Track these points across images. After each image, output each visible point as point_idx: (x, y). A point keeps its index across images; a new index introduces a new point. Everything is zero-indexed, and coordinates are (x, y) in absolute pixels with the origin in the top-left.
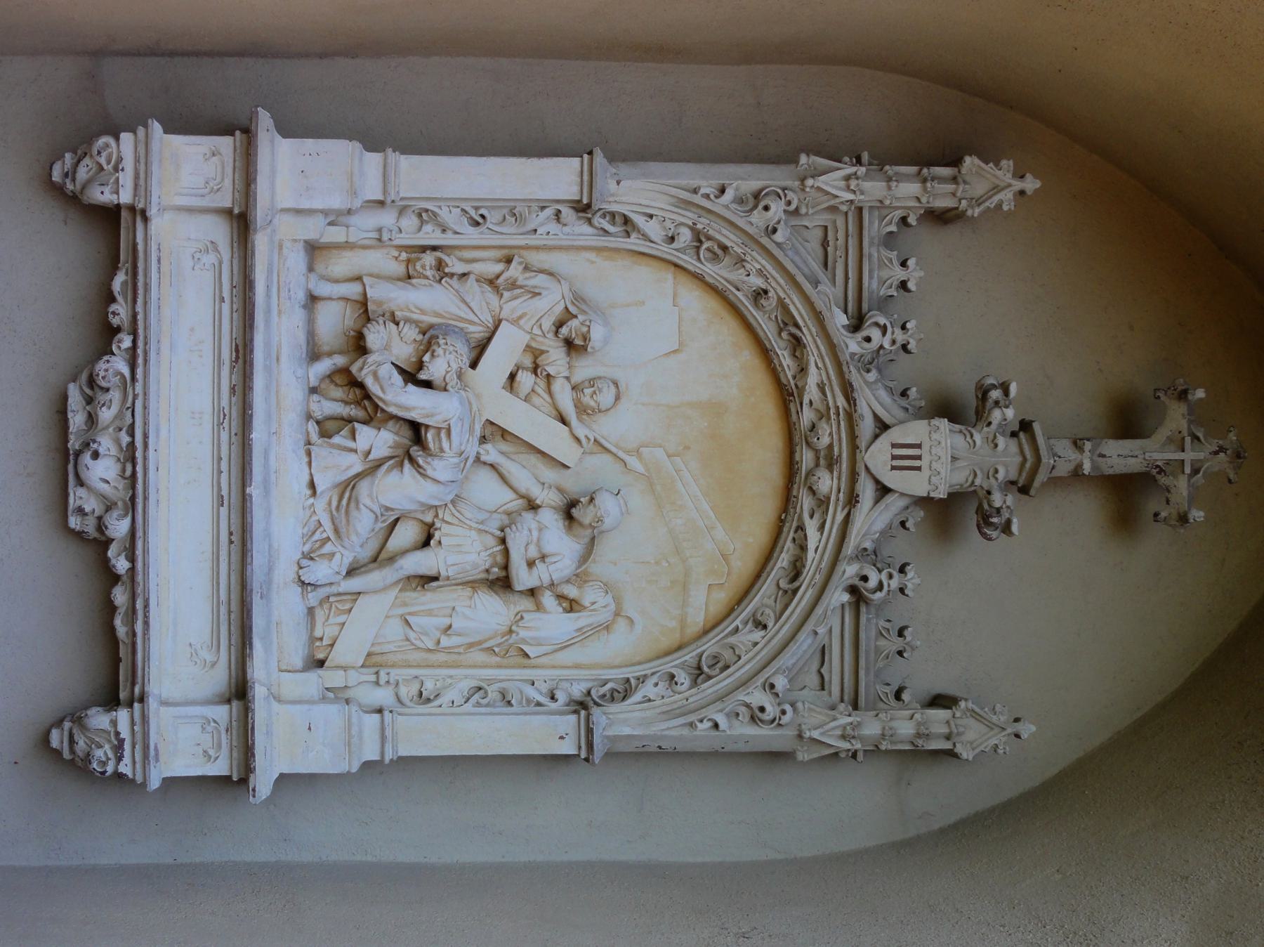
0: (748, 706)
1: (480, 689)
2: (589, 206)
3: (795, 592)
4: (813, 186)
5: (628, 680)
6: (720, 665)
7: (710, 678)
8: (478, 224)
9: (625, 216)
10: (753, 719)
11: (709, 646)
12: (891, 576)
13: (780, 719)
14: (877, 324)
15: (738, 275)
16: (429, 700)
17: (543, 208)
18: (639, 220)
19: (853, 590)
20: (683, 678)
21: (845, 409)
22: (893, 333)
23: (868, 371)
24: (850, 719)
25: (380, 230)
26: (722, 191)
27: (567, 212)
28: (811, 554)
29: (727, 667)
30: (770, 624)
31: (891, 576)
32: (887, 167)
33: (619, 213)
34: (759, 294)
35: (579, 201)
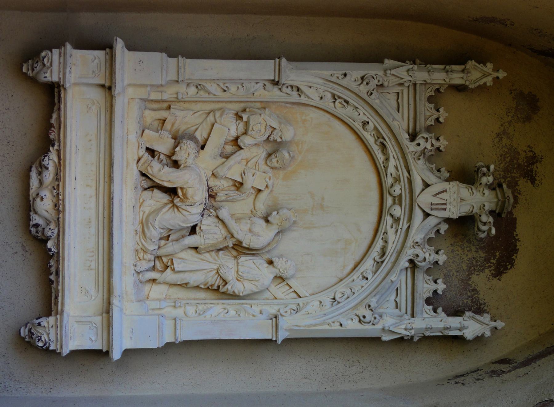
0: (357, 315)
2: (278, 82)
3: (382, 262)
4: (390, 74)
7: (339, 303)
9: (298, 87)
10: (360, 321)
14: (423, 138)
17: (257, 83)
18: (303, 88)
19: (411, 261)
21: (407, 177)
23: (419, 159)
24: (409, 321)
25: (177, 94)
26: (345, 75)
27: (268, 85)
28: (390, 244)
29: (348, 298)
30: (369, 278)
31: (430, 255)
32: (428, 66)
33: (295, 86)
34: (365, 124)
35: (273, 80)
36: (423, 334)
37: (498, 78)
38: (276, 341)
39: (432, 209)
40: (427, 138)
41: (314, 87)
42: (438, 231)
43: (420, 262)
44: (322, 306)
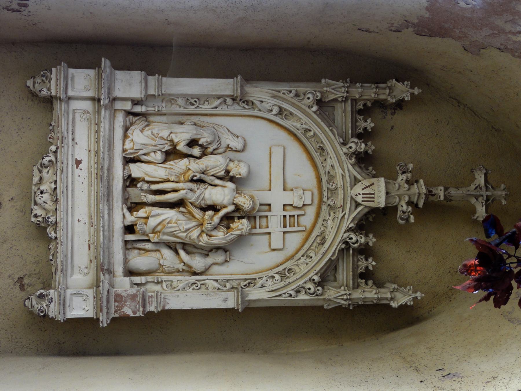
0: (304, 288)
1: (195, 283)
5: (255, 279)
6: (293, 273)
8: (193, 105)
11: (288, 265)
12: (361, 238)
13: (317, 292)
15: (298, 125)
16: (174, 288)
17: (219, 98)
20: (277, 277)
21: (342, 175)
22: (361, 145)
24: (345, 292)
27: (229, 101)
33: (250, 100)
35: (233, 96)
36: (358, 303)
37: (414, 93)
38: (238, 309)
39: (363, 201)
40: (358, 142)
41: (264, 101)
42: (368, 218)
43: (354, 243)
44: (275, 280)
